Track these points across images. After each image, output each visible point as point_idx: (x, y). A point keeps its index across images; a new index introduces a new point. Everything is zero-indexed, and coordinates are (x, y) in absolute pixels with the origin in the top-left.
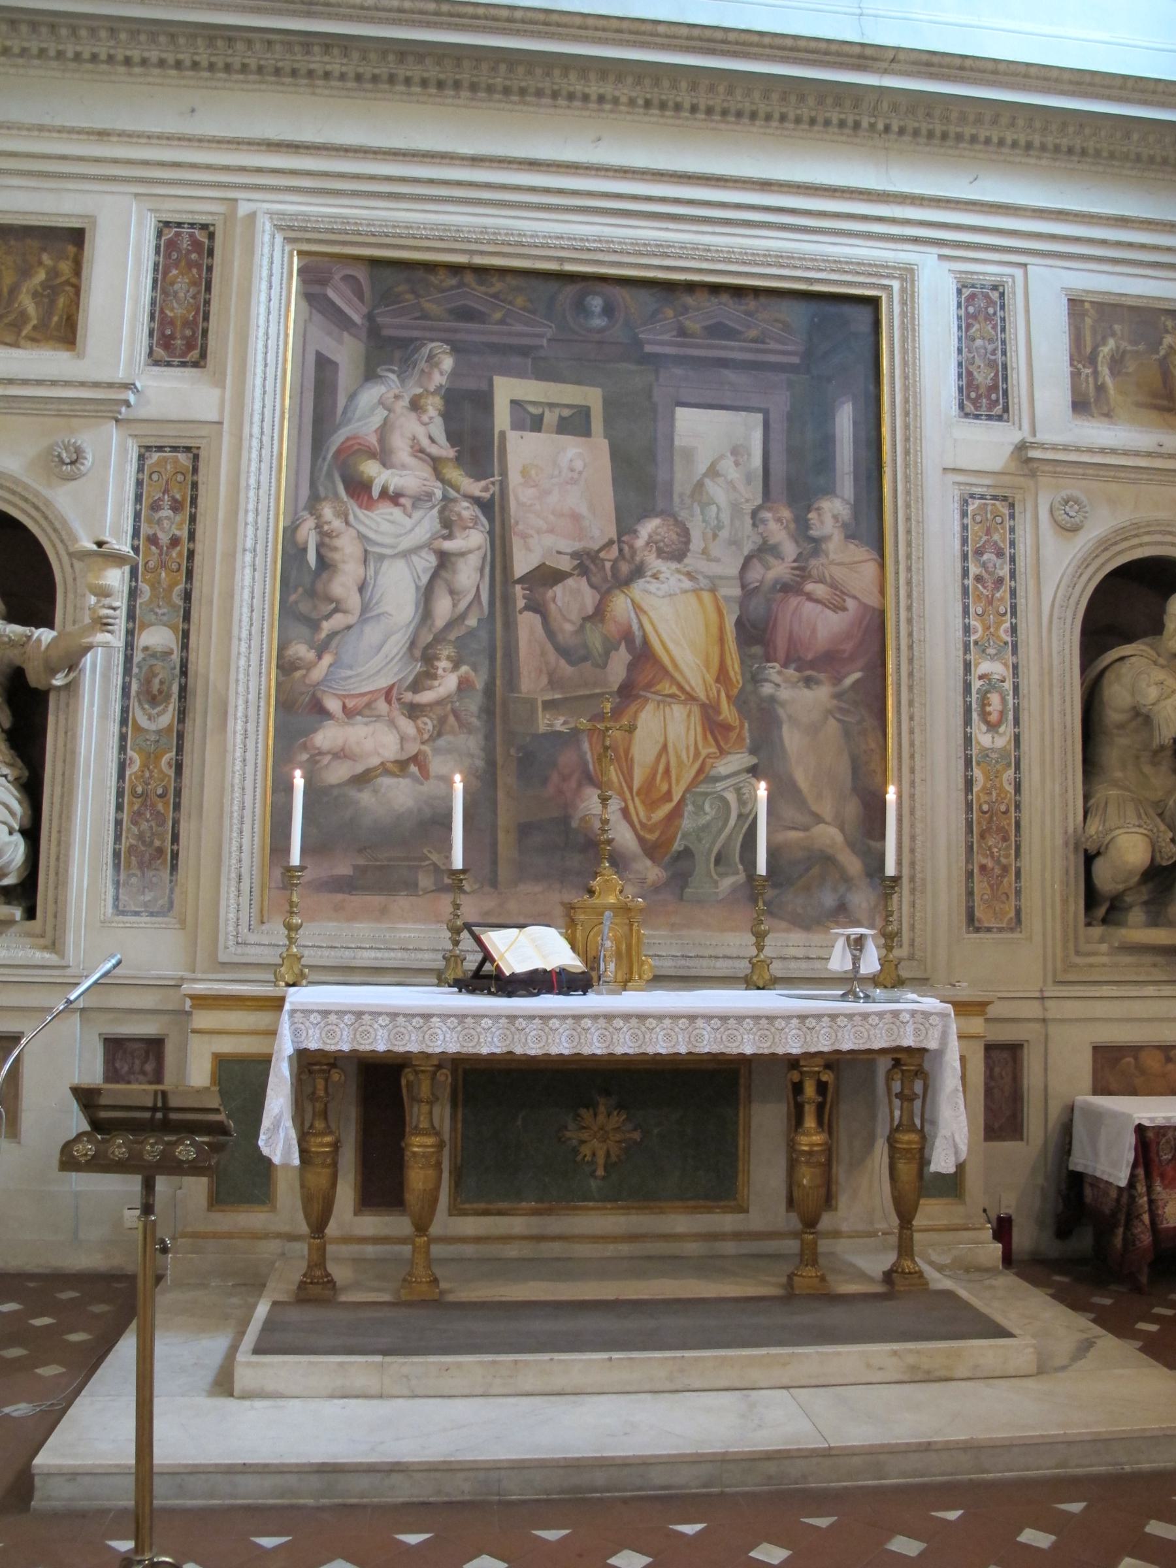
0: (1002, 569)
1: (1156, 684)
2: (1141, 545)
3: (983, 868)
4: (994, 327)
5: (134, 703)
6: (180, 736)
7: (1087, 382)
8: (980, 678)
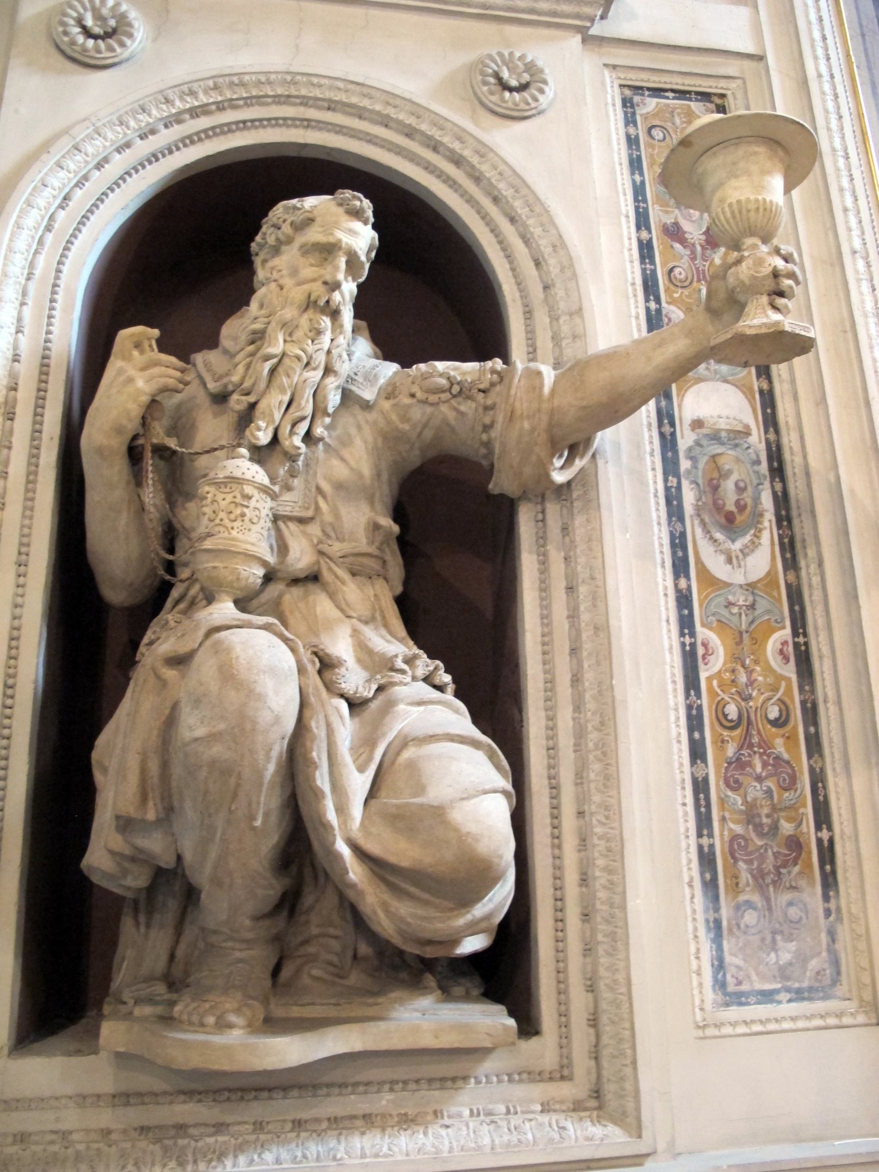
5: (694, 530)
6: (795, 596)
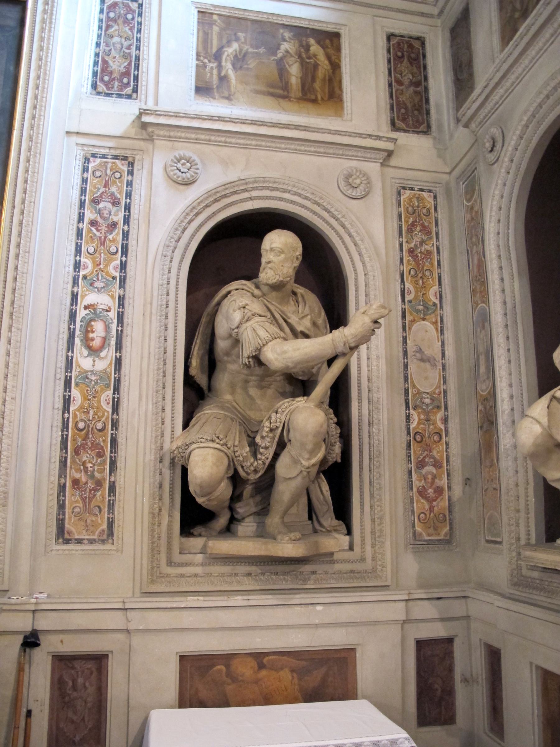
0: (116, 215)
1: (240, 309)
2: (251, 199)
3: (76, 482)
4: (131, 29)
7: (212, 74)
8: (86, 308)
